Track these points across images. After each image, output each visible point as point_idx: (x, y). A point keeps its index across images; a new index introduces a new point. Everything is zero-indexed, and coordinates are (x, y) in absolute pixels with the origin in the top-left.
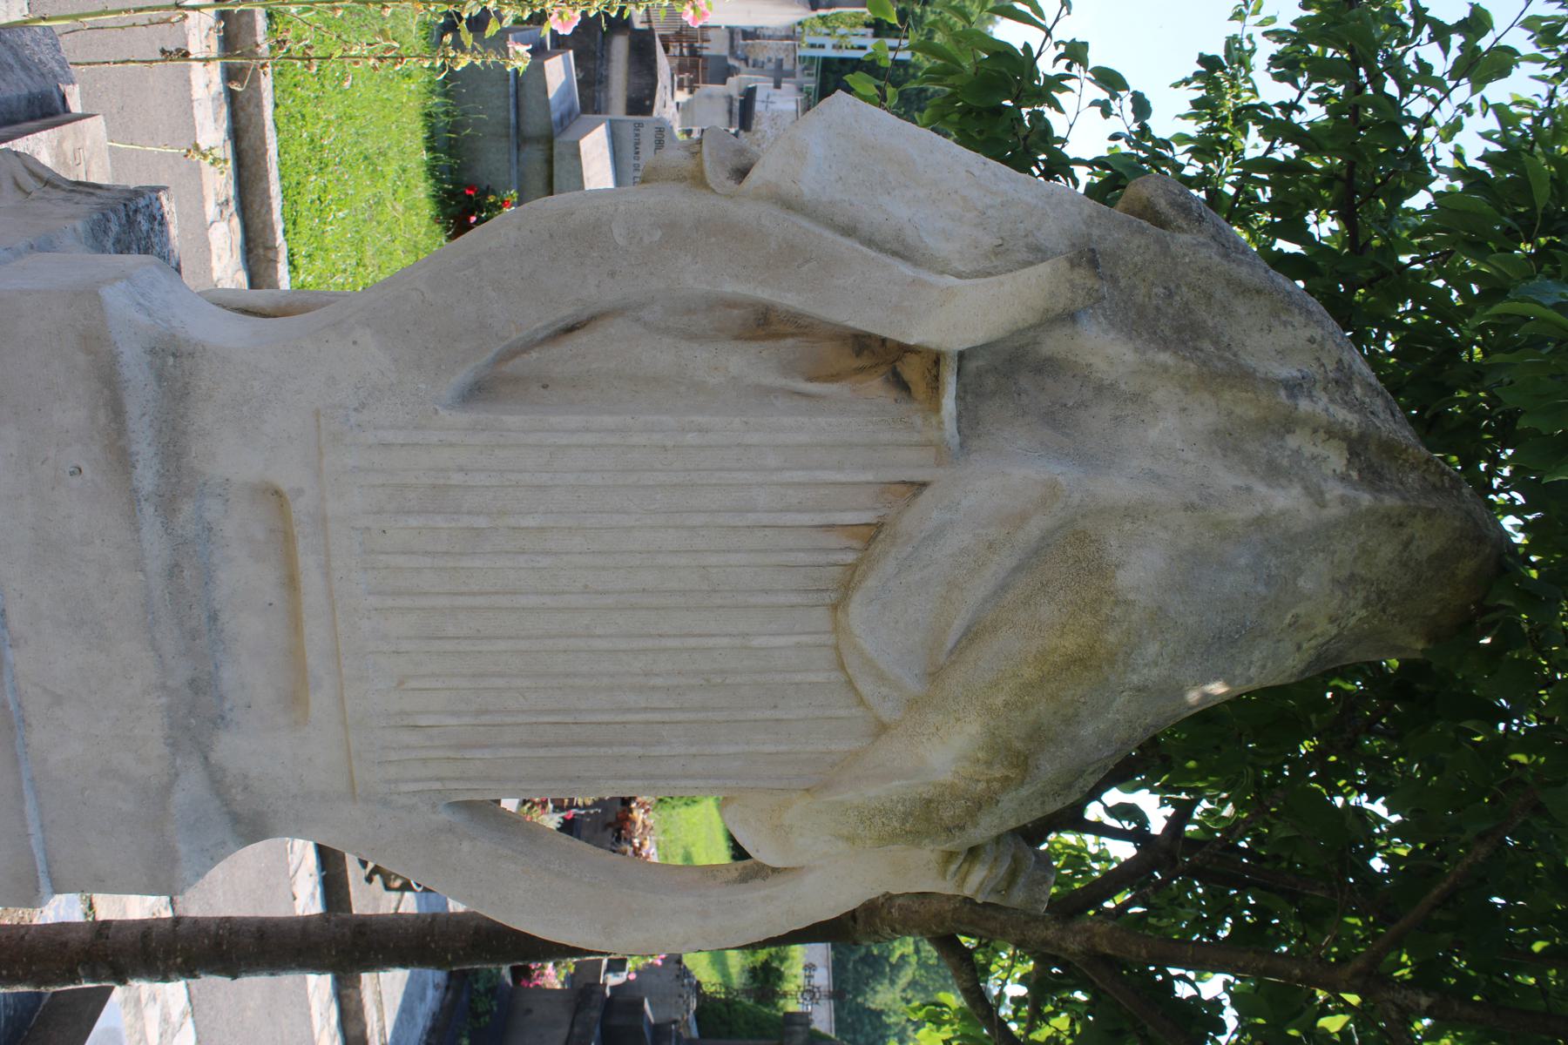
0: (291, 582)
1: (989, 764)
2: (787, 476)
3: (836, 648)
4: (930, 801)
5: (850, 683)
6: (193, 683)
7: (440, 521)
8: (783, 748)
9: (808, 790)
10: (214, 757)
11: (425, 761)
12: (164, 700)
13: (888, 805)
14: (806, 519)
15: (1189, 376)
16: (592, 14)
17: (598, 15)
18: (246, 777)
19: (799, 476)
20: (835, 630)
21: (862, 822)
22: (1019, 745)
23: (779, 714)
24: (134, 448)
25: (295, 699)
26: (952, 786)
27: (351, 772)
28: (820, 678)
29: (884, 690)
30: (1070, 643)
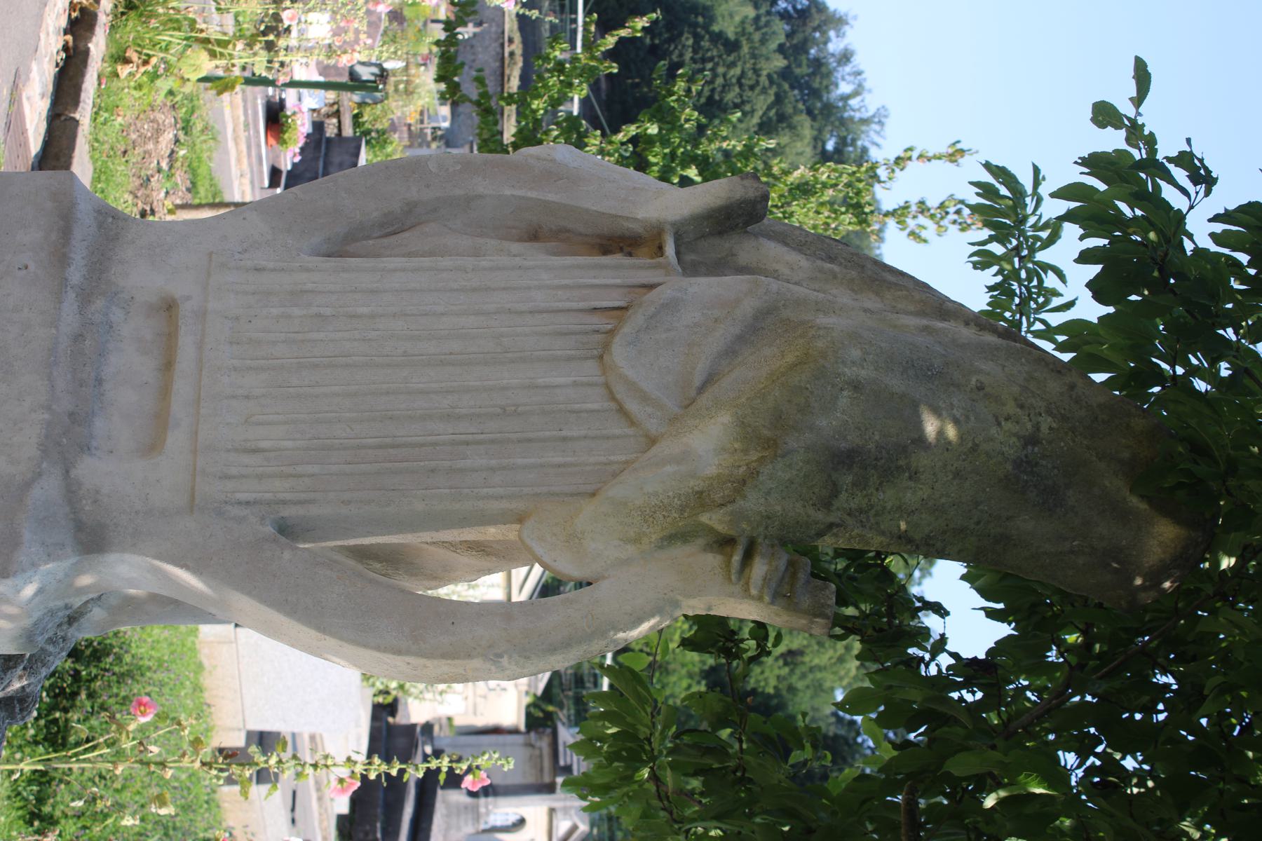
0: (168, 365)
1: (745, 451)
2: (556, 282)
3: (607, 386)
4: (701, 493)
5: (622, 411)
6: (71, 414)
7: (296, 311)
8: (569, 459)
9: (593, 495)
10: (73, 473)
11: (260, 477)
12: (46, 416)
13: (666, 501)
14: (574, 305)
15: (853, 280)
16: (372, 776)
17: (379, 776)
18: (97, 492)
20: (604, 374)
21: (646, 521)
23: (564, 433)
24: (72, 255)
25: (152, 446)
26: (718, 476)
27: (193, 489)
29: (649, 410)
30: (790, 358)
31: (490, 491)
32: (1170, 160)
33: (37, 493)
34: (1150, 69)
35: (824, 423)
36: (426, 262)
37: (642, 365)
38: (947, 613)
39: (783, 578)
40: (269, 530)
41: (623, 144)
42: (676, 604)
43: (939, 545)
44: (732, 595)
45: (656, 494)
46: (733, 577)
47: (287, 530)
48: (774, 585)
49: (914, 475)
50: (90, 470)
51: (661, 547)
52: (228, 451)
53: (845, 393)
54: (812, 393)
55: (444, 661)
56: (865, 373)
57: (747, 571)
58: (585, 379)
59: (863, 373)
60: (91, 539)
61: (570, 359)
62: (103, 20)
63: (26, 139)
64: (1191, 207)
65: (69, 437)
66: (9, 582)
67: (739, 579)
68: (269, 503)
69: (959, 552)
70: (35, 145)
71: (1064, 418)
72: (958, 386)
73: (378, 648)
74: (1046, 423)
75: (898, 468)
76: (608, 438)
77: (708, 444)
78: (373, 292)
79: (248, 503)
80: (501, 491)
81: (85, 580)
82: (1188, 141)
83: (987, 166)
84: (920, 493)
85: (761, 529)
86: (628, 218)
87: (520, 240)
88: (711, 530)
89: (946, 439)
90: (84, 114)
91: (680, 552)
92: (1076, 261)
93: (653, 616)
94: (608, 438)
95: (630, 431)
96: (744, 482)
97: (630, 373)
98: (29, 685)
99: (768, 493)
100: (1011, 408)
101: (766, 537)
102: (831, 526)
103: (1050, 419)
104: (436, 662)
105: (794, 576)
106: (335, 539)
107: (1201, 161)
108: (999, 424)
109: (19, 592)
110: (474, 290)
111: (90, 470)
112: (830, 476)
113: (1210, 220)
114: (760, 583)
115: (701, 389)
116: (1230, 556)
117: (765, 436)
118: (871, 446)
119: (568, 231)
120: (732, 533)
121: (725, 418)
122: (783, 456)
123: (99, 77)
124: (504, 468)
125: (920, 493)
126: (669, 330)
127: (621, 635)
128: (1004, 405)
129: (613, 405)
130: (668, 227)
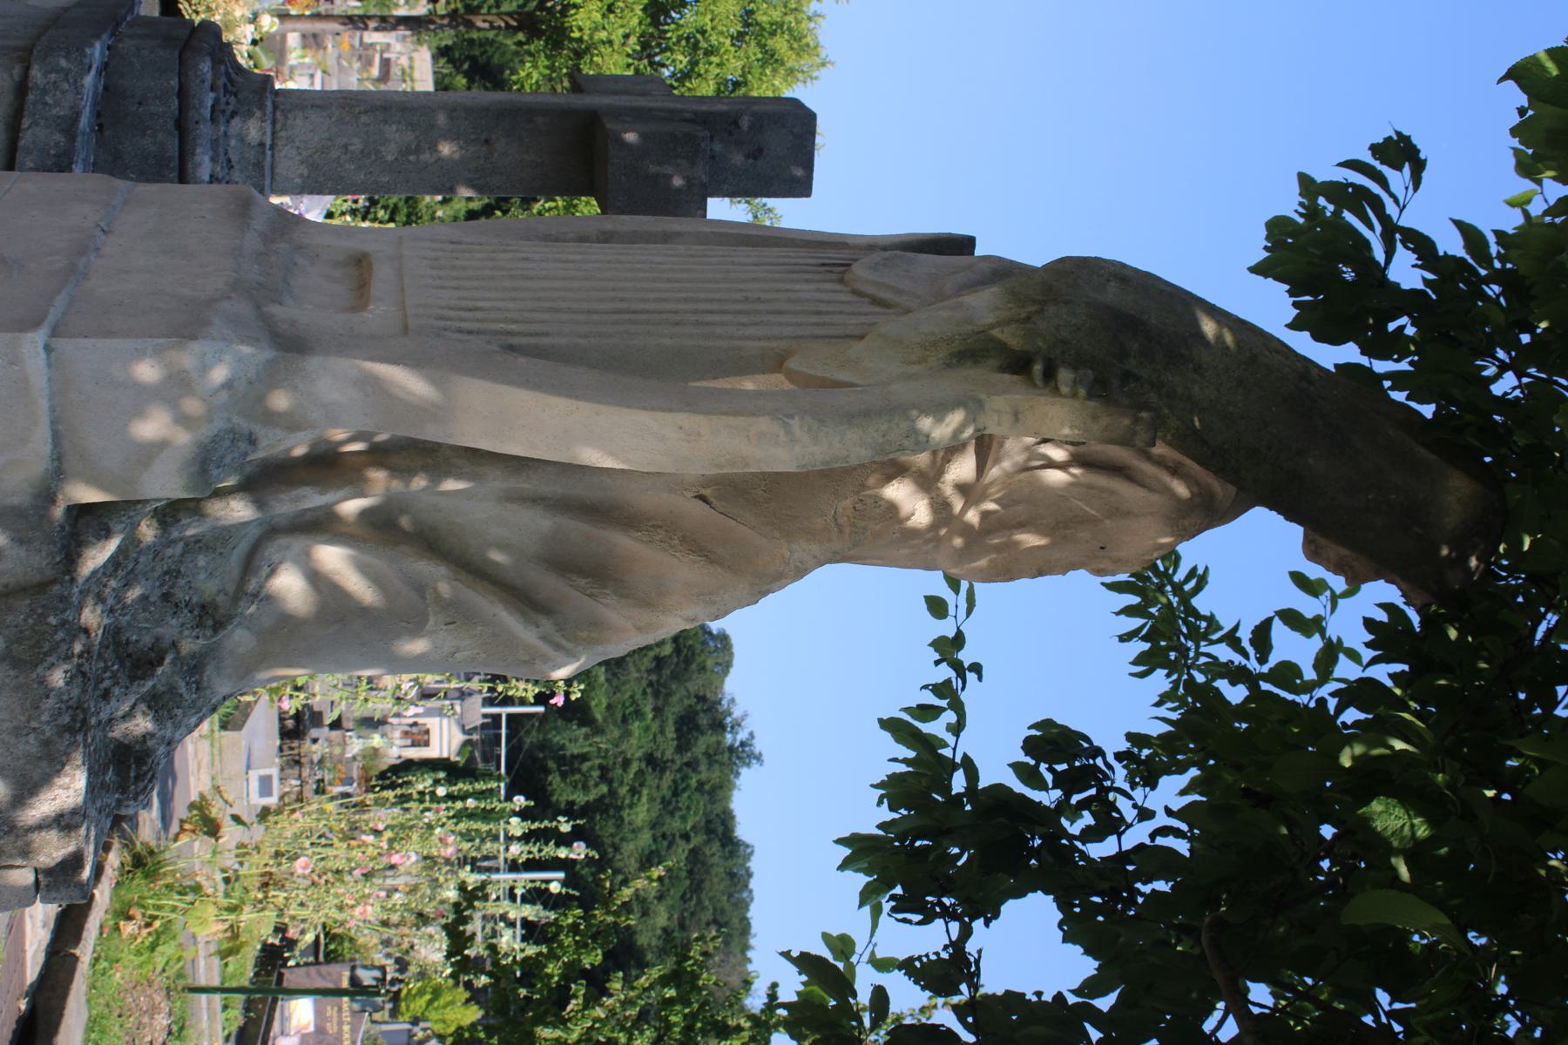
9: (862, 337)
32: (1374, 149)
41: (645, 990)
45: (933, 334)
51: (948, 366)
62: (110, 873)
63: (23, 964)
66: (196, 346)
70: (32, 973)
88: (1002, 347)
89: (1224, 342)
90: (85, 952)
98: (152, 735)
109: (205, 369)
123: (101, 927)
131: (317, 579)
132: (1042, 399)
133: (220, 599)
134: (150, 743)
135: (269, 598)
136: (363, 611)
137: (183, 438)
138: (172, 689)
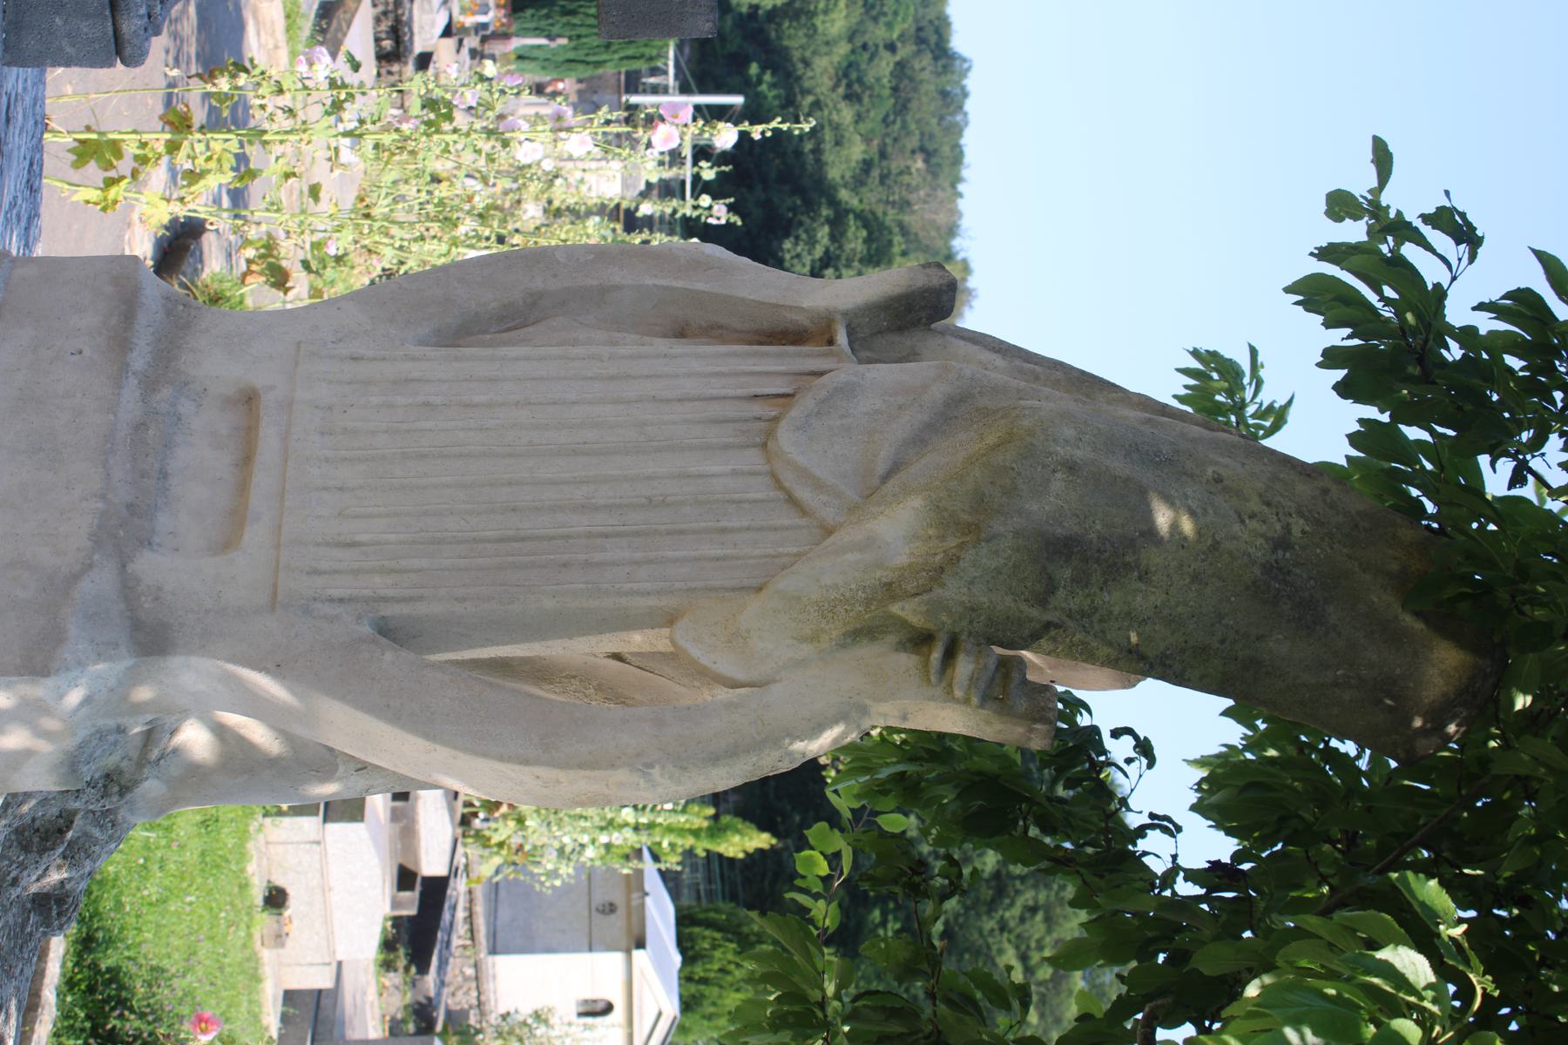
0: (246, 460)
2: (709, 369)
3: (774, 476)
4: (890, 584)
5: (792, 500)
6: (130, 506)
9: (760, 589)
10: (130, 568)
11: (356, 572)
12: (100, 505)
14: (731, 392)
18: (160, 589)
19: (718, 369)
20: (769, 461)
21: (824, 617)
22: (965, 517)
23: (723, 524)
25: (227, 543)
27: (275, 586)
28: (759, 496)
29: (824, 498)
30: (991, 439)
31: (635, 586)
32: (1426, 218)
33: (86, 586)
34: (1391, 148)
35: (1035, 508)
36: (555, 351)
37: (815, 451)
38: (1179, 829)
39: (993, 679)
40: (366, 629)
42: (864, 711)
43: (1177, 667)
44: (932, 698)
45: (836, 587)
46: (933, 678)
47: (388, 631)
48: (982, 685)
49: (1145, 576)
50: (148, 565)
51: (843, 646)
52: (318, 545)
53: (1059, 475)
54: (1019, 474)
55: (582, 773)
56: (1080, 454)
57: (949, 671)
58: (746, 468)
59: (1079, 454)
60: (151, 638)
61: (727, 447)
64: (1454, 279)
65: (126, 528)
66: (50, 682)
67: (940, 681)
68: (366, 600)
69: (1201, 679)
71: (1318, 523)
72: (1192, 476)
73: (501, 758)
74: (1298, 526)
75: (1126, 565)
76: (775, 529)
77: (897, 531)
78: (492, 380)
79: (341, 600)
80: (648, 586)
81: (143, 694)
82: (1447, 193)
83: (1195, 353)
84: (1152, 598)
85: (964, 623)
86: (791, 308)
87: (665, 336)
88: (903, 624)
89: (1181, 533)
91: (868, 652)
92: (1319, 365)
93: (837, 722)
94: (775, 529)
95: (803, 522)
96: (942, 570)
97: (801, 460)
98: (70, 879)
99: (972, 583)
100: (1255, 505)
101: (970, 634)
102: (1048, 626)
103: (1302, 521)
104: (572, 774)
105: (1007, 676)
106: (447, 650)
107: (1463, 215)
108: (1243, 522)
109: (61, 697)
110: (612, 378)
111: (148, 565)
112: (1044, 568)
113: (1474, 309)
114: (966, 683)
115: (885, 478)
116: (1525, 693)
117: (965, 521)
118: (1092, 535)
119: (720, 327)
120: (930, 626)
121: (916, 502)
122: (988, 541)
124: (651, 562)
125: (1152, 598)
126: (843, 416)
127: (799, 746)
128: (1247, 500)
129: (781, 495)
130: (838, 317)
131: (221, 732)
132: (932, 704)
133: (124, 764)
134: (68, 887)
135: (175, 751)
136: (272, 762)
137: (44, 747)
138: (86, 834)
